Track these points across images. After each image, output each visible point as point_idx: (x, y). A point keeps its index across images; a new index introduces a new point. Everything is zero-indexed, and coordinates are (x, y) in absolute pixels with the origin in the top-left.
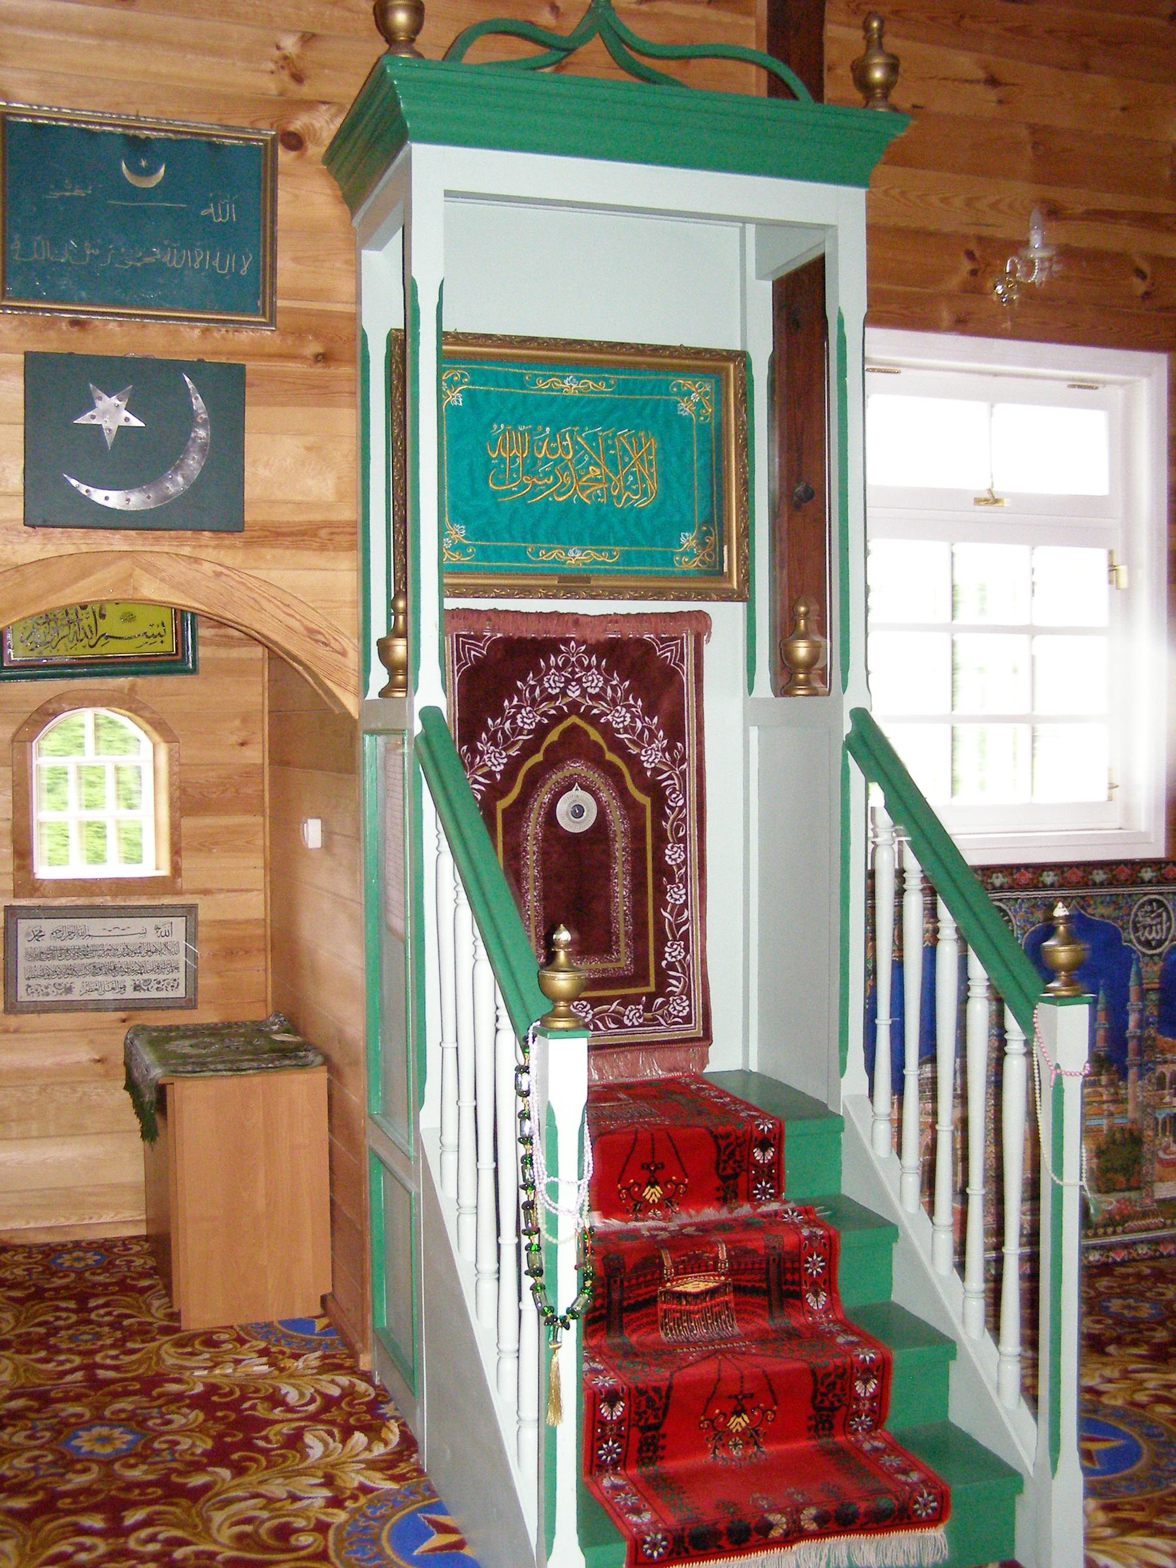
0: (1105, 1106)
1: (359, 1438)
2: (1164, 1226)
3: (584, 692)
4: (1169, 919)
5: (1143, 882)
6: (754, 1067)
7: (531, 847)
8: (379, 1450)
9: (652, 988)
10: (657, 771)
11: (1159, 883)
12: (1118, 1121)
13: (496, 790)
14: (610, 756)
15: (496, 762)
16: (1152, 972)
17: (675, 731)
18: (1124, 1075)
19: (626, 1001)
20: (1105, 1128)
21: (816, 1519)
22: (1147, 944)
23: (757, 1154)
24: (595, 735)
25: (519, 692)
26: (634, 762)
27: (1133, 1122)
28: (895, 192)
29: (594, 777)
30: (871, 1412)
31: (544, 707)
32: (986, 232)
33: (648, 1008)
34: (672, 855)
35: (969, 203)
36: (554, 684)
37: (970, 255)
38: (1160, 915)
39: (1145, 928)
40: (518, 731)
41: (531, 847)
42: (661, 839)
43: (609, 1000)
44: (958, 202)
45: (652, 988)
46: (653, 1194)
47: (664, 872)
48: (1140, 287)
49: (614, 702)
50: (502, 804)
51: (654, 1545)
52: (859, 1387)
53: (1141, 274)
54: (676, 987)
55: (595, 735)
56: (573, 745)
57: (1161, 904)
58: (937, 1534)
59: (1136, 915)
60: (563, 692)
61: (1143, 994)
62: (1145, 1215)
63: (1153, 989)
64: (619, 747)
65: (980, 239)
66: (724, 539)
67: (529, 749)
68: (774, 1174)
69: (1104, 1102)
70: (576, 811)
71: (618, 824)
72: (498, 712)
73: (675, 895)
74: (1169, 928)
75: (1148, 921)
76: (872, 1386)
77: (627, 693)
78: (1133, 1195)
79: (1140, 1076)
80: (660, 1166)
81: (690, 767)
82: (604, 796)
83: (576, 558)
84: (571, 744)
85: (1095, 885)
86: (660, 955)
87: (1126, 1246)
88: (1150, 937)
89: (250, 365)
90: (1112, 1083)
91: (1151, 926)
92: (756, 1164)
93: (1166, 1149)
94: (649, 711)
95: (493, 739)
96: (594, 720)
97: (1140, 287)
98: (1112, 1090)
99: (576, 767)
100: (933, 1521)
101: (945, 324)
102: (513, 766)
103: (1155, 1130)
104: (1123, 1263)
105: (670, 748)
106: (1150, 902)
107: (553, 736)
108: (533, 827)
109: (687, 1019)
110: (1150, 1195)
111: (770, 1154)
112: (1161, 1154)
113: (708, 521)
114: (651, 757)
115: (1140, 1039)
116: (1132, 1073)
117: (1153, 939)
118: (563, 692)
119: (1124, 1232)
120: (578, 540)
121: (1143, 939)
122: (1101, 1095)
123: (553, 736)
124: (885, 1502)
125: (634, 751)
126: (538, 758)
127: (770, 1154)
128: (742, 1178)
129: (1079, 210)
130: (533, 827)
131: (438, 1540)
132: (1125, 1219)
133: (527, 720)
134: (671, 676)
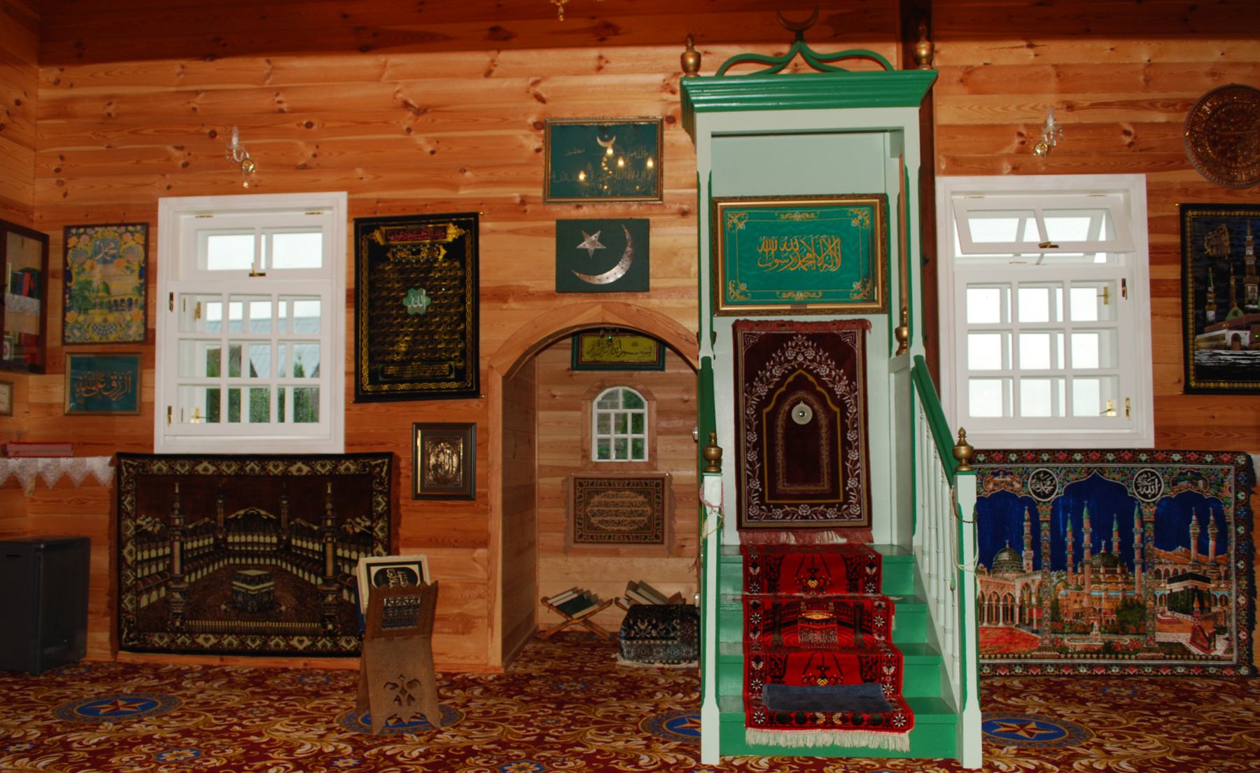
1: (680, 695)
2: (1164, 658)
3: (805, 358)
4: (1159, 482)
5: (1141, 461)
6: (895, 542)
7: (780, 431)
8: (687, 699)
9: (841, 500)
10: (843, 396)
11: (1152, 462)
12: (1129, 594)
13: (763, 403)
14: (819, 388)
15: (762, 390)
16: (1149, 512)
17: (852, 377)
18: (1132, 569)
19: (828, 506)
21: (841, 719)
22: (1145, 496)
23: (868, 570)
24: (811, 379)
25: (774, 359)
26: (831, 392)
27: (1139, 595)
28: (976, 108)
29: (811, 398)
30: (892, 683)
31: (786, 365)
32: (1029, 121)
33: (839, 510)
34: (851, 436)
35: (1018, 108)
36: (790, 355)
37: (1020, 134)
40: (773, 376)
41: (780, 431)
42: (845, 429)
43: (819, 505)
44: (1012, 108)
45: (841, 500)
46: (813, 584)
47: (847, 445)
48: (1127, 140)
49: (820, 363)
50: (766, 410)
51: (759, 718)
52: (885, 669)
53: (1127, 133)
54: (853, 500)
55: (811, 379)
56: (800, 384)
57: (1153, 474)
58: (905, 736)
60: (795, 358)
61: (1143, 524)
62: (1150, 650)
64: (823, 384)
65: (1026, 126)
66: (875, 284)
67: (778, 385)
68: (876, 579)
70: (802, 414)
71: (823, 421)
72: (764, 368)
73: (853, 455)
76: (892, 670)
77: (827, 358)
78: (1141, 638)
79: (1143, 570)
80: (817, 570)
81: (860, 393)
82: (816, 407)
83: (800, 296)
84: (801, 384)
85: (1108, 461)
86: (845, 484)
87: (1138, 666)
89: (652, 219)
90: (1123, 572)
92: (867, 575)
93: (1162, 613)
94: (838, 367)
95: (761, 380)
96: (810, 372)
97: (1127, 140)
99: (801, 394)
100: (902, 730)
101: (1006, 171)
102: (771, 393)
104: (1134, 675)
105: (849, 385)
106: (1146, 472)
107: (791, 379)
108: (780, 421)
109: (859, 516)
110: (1153, 639)
111: (874, 570)
113: (867, 276)
114: (840, 389)
115: (1142, 550)
116: (1138, 568)
118: (795, 358)
120: (802, 289)
123: (791, 379)
124: (877, 716)
125: (831, 386)
126: (783, 389)
127: (874, 570)
128: (860, 582)
129: (1087, 104)
130: (780, 421)
131: (689, 725)
132: (1136, 651)
133: (777, 372)
134: (851, 351)
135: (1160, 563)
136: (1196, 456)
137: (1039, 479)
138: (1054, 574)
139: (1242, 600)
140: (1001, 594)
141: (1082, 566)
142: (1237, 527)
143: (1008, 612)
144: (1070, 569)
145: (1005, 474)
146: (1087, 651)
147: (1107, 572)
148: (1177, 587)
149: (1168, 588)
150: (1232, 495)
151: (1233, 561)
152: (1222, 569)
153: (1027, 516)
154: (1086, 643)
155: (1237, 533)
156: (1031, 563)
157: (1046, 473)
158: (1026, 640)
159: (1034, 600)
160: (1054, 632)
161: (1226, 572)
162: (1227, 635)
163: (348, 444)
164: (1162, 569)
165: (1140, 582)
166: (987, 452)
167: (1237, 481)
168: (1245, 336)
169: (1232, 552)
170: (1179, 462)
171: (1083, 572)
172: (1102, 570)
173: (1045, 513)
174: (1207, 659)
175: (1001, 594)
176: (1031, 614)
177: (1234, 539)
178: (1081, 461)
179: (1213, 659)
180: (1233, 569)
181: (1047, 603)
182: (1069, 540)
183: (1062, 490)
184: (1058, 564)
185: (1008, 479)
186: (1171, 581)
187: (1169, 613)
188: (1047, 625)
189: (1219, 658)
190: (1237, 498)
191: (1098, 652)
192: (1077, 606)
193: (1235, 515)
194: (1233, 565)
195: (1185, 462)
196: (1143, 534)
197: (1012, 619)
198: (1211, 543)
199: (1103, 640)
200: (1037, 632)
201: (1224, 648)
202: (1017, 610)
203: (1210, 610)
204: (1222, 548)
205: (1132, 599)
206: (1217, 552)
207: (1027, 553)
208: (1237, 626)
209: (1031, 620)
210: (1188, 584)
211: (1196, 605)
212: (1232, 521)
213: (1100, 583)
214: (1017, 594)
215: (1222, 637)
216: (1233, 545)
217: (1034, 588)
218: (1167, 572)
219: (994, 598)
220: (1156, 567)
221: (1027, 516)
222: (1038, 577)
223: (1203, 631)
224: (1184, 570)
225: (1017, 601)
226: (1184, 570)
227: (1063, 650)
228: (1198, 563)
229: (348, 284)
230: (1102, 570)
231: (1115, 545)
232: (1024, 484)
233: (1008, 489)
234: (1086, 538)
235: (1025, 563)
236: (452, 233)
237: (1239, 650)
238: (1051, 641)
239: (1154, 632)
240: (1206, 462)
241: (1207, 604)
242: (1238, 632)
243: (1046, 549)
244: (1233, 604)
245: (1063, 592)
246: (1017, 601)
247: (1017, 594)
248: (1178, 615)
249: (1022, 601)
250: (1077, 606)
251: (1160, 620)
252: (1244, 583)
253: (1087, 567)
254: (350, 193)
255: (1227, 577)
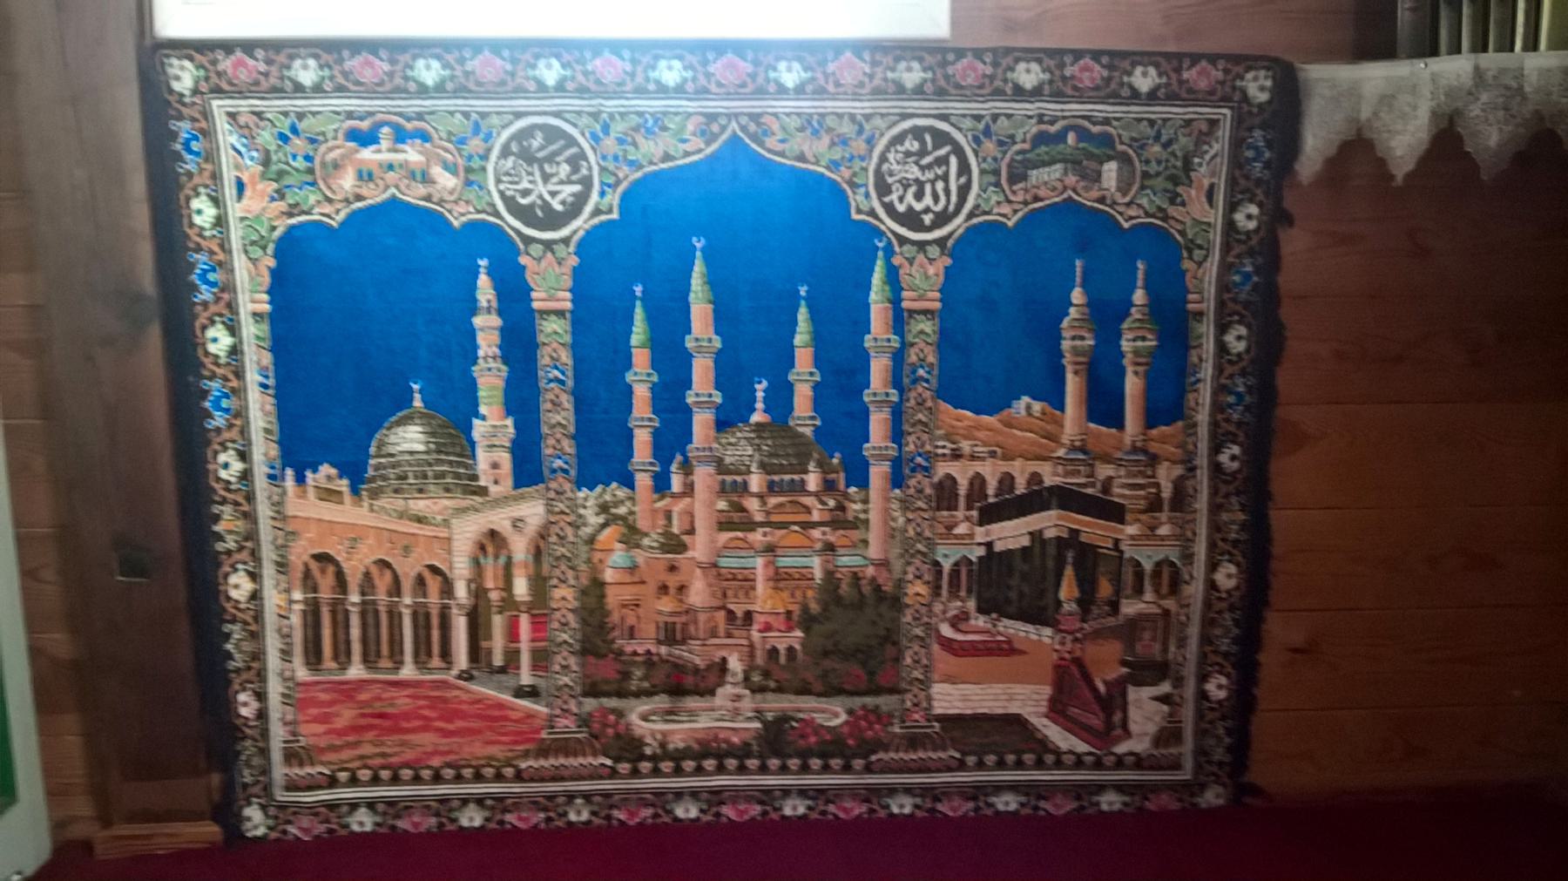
0: (816, 533)
4: (964, 168)
12: (846, 561)
20: (818, 574)
22: (911, 219)
27: (884, 564)
38: (944, 161)
39: (906, 187)
57: (941, 138)
59: (883, 159)
61: (900, 319)
62: (913, 742)
63: (925, 312)
69: (814, 525)
74: (964, 191)
75: (914, 172)
78: (885, 702)
79: (897, 480)
88: (918, 207)
90: (829, 486)
91: (920, 184)
98: (832, 503)
103: (936, 590)
106: (917, 133)
112: (946, 631)
115: (897, 414)
116: (878, 473)
117: (927, 210)
119: (868, 769)
121: (901, 208)
122: (808, 510)
135: (956, 455)
136: (1099, 72)
137: (528, 157)
138: (588, 499)
139: (1227, 577)
140: (408, 569)
141: (687, 469)
142: (1222, 328)
143: (431, 636)
144: (643, 480)
145: (400, 136)
146: (709, 751)
147: (772, 488)
148: (1011, 534)
149: (969, 539)
150: (1216, 217)
151: (1203, 447)
152: (1166, 476)
153: (485, 291)
154: (704, 723)
155: (1222, 348)
156: (505, 458)
157: (552, 134)
158: (493, 715)
159: (521, 588)
160: (593, 691)
161: (1179, 485)
162: (1165, 688)
164: (962, 473)
165: (887, 515)
166: (329, 49)
167: (1237, 163)
169: (1203, 417)
170: (1036, 93)
171: (689, 490)
172: (756, 482)
173: (550, 286)
174: (1098, 765)
175: (408, 569)
176: (513, 634)
177: (1207, 371)
178: (680, 90)
179: (1120, 763)
180: (1203, 477)
181: (564, 595)
182: (641, 379)
183: (613, 198)
184: (603, 457)
185: (412, 154)
186: (990, 515)
187: (981, 622)
188: (567, 670)
189: (1139, 762)
190: (1230, 226)
191: (743, 752)
192: (666, 605)
193: (1223, 287)
194: (1202, 461)
195: (1058, 96)
196: (898, 357)
197: (446, 654)
198: (1132, 385)
199: (759, 714)
200: (532, 693)
201: (1152, 728)
202: (460, 625)
203: (1114, 606)
204: (1166, 406)
205: (856, 578)
206: (1152, 418)
207: (492, 426)
208: (1203, 658)
209: (512, 657)
210: (1050, 522)
211: (1068, 590)
212: (1210, 306)
213: (751, 526)
214: (461, 569)
215: (1147, 692)
216: (1205, 394)
217: (520, 548)
218: (978, 482)
219: (383, 582)
220: (942, 469)
221: (485, 291)
222: (533, 511)
223: (1088, 679)
224: (1035, 478)
225: (461, 591)
226: (1035, 478)
227: (629, 749)
228: (1085, 453)
230: (756, 482)
231: (803, 396)
232: (471, 176)
233: (413, 195)
234: (702, 371)
235: (483, 459)
237: (1200, 733)
238: (584, 721)
239: (925, 684)
240: (1135, 95)
241: (1105, 589)
242: (1203, 678)
243: (558, 414)
244: (1195, 590)
245: (619, 557)
246: (461, 591)
247: (461, 569)
248: (1013, 628)
249: (479, 593)
250: (666, 605)
251: (947, 644)
252: (1235, 516)
253: (703, 476)
255: (1181, 499)
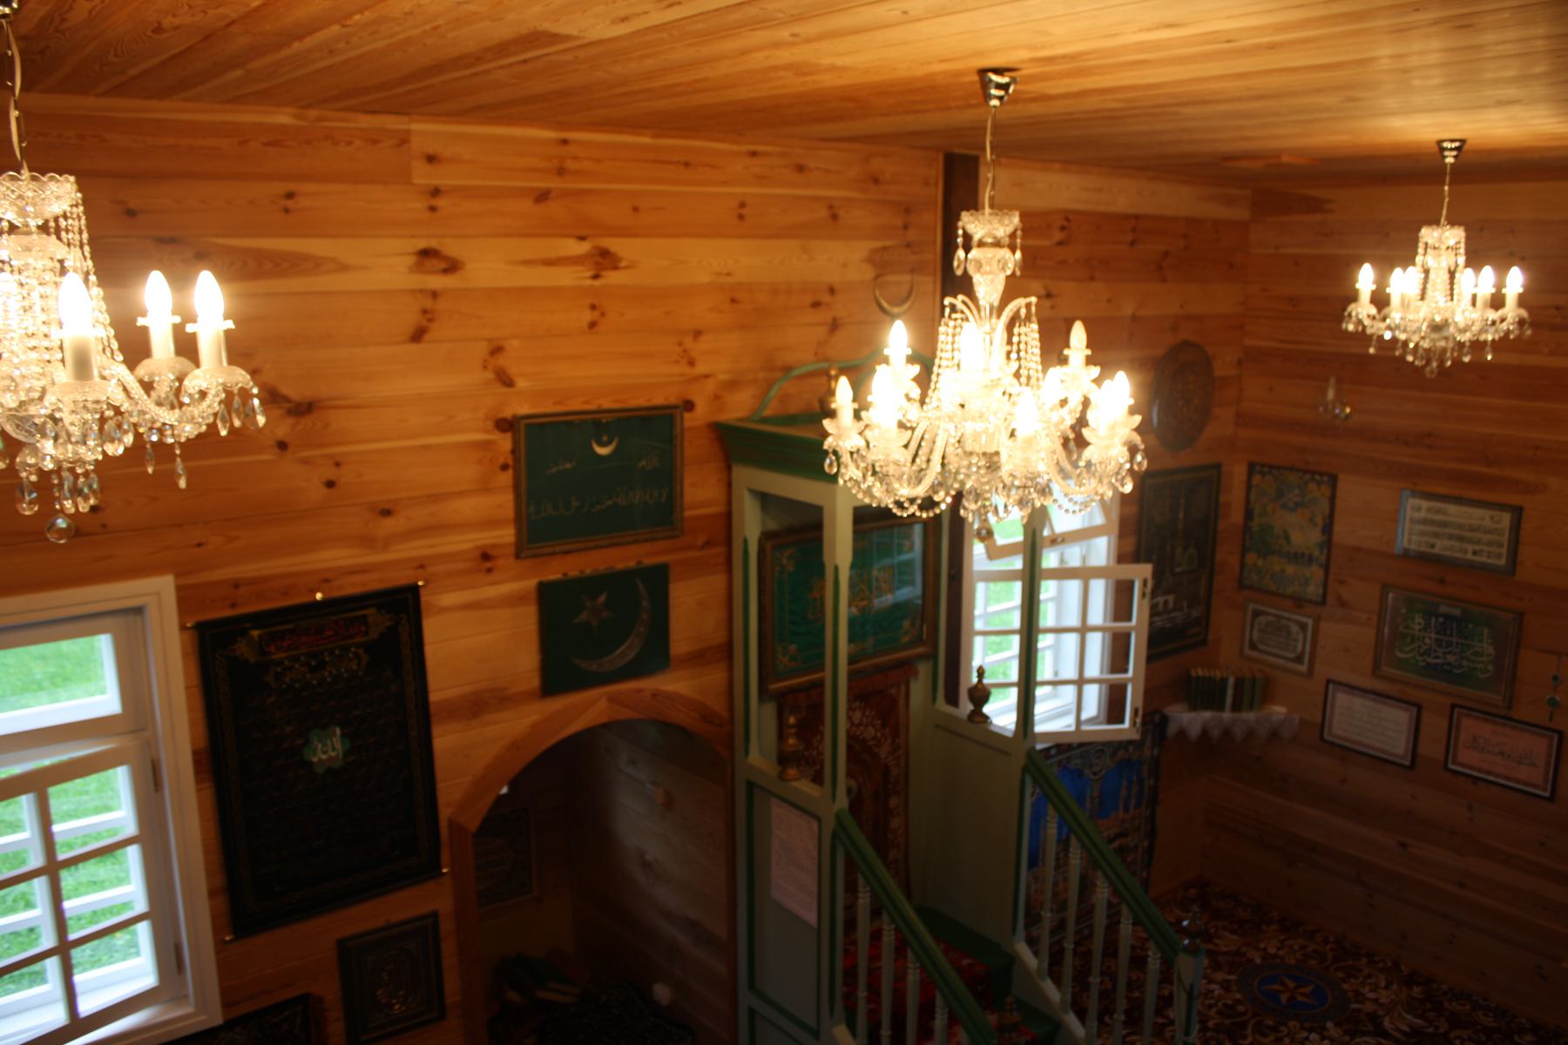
163: (227, 1004)
168: (1171, 598)
229: (193, 741)
236: (379, 622)
254: (178, 576)
